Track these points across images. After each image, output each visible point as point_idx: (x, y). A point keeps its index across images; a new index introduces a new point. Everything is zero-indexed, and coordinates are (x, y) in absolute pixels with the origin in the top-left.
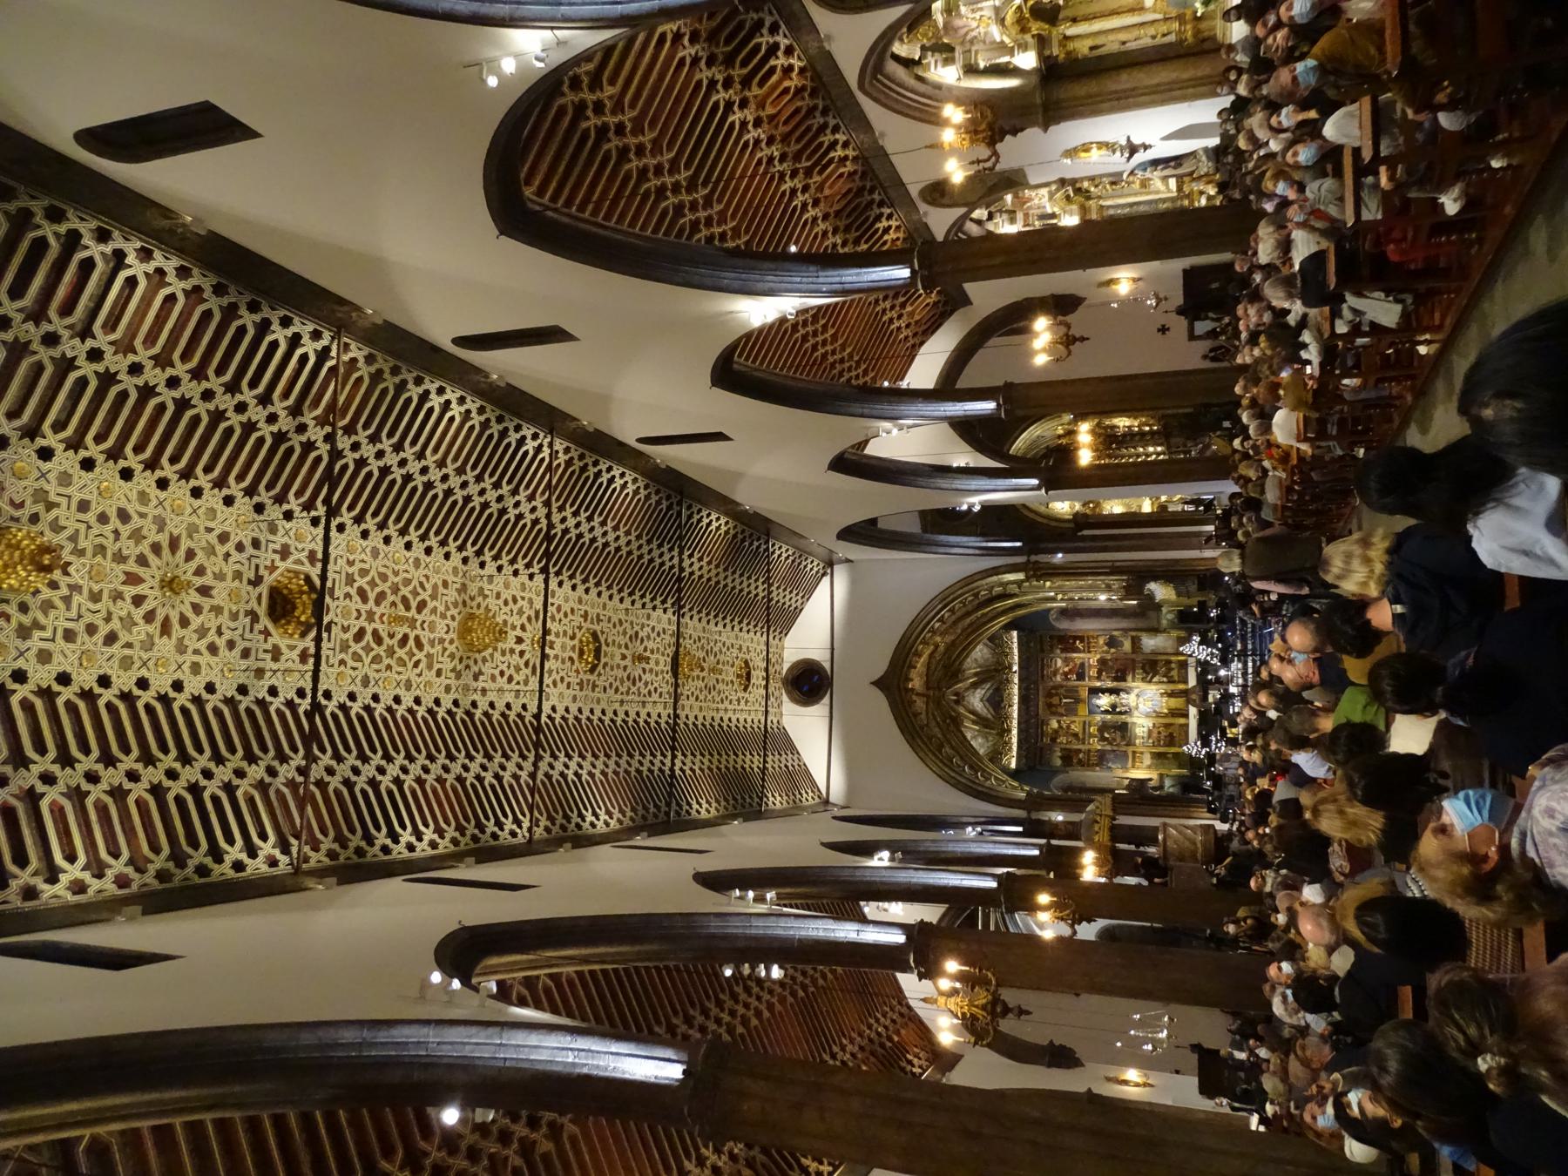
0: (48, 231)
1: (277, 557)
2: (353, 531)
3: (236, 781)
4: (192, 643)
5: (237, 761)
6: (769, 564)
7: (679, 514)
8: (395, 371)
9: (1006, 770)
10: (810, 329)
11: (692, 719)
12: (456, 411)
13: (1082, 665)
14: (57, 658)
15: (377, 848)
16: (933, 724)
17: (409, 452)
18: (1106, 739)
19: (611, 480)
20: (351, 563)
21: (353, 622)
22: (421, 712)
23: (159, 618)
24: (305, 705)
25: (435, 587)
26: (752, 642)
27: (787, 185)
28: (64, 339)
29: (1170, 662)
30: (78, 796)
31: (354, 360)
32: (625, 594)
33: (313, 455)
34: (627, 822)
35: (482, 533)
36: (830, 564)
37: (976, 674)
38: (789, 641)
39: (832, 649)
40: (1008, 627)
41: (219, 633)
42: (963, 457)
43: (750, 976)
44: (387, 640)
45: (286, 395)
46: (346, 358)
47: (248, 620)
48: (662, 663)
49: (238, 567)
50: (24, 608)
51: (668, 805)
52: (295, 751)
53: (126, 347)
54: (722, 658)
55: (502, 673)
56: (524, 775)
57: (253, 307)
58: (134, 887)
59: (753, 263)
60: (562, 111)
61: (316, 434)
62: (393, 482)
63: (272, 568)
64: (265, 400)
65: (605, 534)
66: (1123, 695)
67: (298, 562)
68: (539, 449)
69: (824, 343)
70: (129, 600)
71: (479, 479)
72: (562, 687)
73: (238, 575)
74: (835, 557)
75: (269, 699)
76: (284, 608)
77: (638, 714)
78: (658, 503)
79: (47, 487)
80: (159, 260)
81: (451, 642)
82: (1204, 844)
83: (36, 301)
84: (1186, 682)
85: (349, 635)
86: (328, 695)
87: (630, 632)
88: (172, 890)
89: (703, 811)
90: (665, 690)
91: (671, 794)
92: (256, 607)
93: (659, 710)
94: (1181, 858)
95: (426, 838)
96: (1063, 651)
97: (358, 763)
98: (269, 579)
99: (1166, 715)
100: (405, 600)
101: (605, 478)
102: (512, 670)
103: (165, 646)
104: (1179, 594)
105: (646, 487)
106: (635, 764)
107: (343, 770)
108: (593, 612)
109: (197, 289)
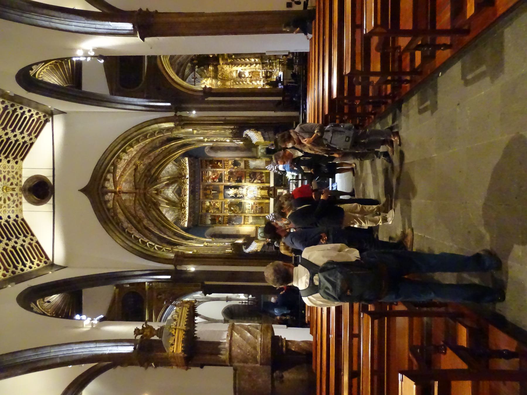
13: (221, 174)
18: (232, 210)
29: (262, 173)
36: (51, 114)
37: (168, 180)
40: (184, 155)
66: (240, 189)
82: (263, 346)
84: (269, 183)
96: (212, 167)
99: (260, 199)
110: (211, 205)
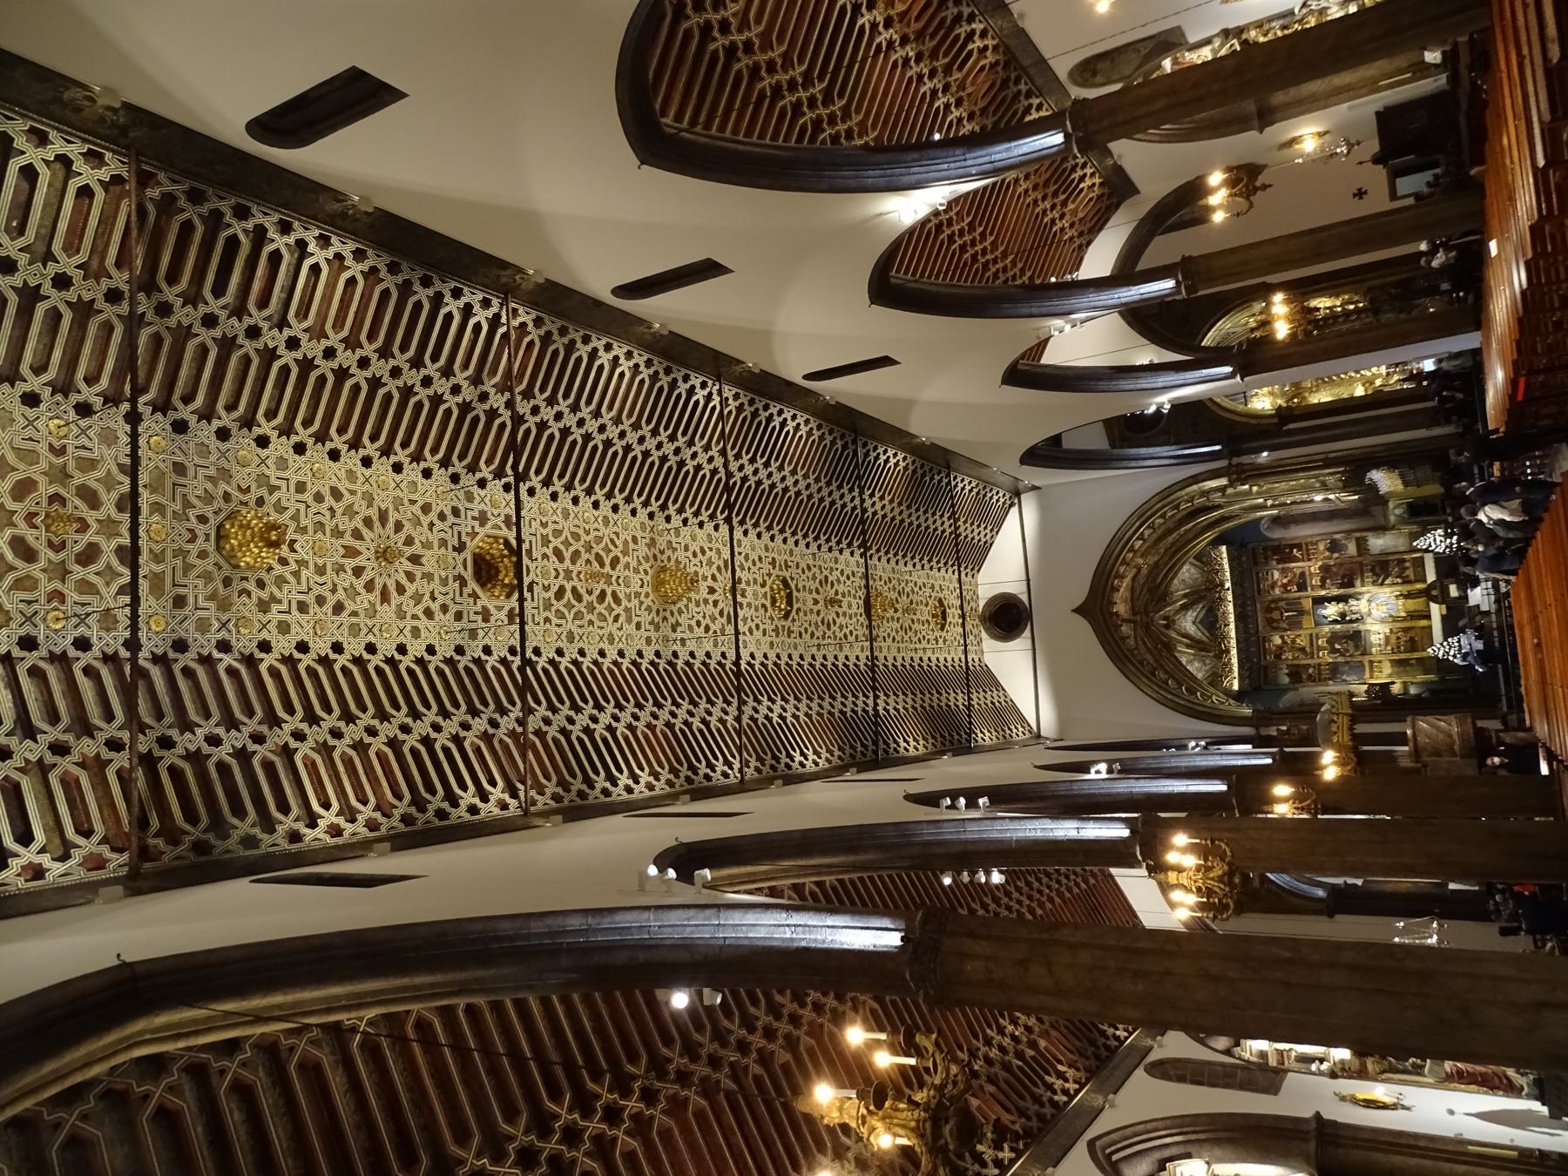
0: (239, 229)
1: (476, 523)
2: (543, 494)
3: (463, 734)
4: (410, 609)
5: (461, 714)
6: (952, 498)
7: (855, 452)
8: (563, 331)
9: (1228, 693)
10: (967, 238)
11: (891, 660)
12: (625, 366)
13: (1303, 574)
14: (294, 629)
15: (598, 791)
16: (1143, 650)
17: (585, 412)
19: (783, 424)
20: (545, 525)
21: (552, 581)
22: (626, 663)
23: (378, 587)
24: (516, 662)
25: (626, 542)
26: (944, 580)
27: (927, 86)
28: (264, 331)
29: (1404, 561)
30: (325, 750)
31: (523, 325)
32: (810, 539)
33: (497, 422)
34: (835, 761)
35: (664, 487)
36: (1018, 494)
37: (1185, 596)
38: (982, 577)
39: (1028, 580)
40: (1216, 542)
41: (434, 599)
42: (1148, 354)
43: (971, 882)
44: (586, 597)
45: (465, 366)
46: (515, 323)
47: (457, 584)
48: (854, 606)
49: (442, 535)
50: (261, 584)
51: (875, 743)
52: (514, 704)
53: (318, 333)
54: (915, 598)
55: (699, 624)
56: (730, 719)
57: (426, 282)
58: (383, 830)
59: (896, 157)
60: (688, 34)
61: (497, 401)
62: (574, 442)
63: (474, 534)
64: (447, 372)
65: (783, 479)
66: (1352, 602)
67: (496, 527)
68: (709, 398)
69: (984, 252)
70: (350, 572)
71: (655, 433)
72: (758, 634)
73: (443, 543)
74: (1021, 486)
75: (484, 657)
76: (488, 572)
77: (836, 657)
78: (833, 443)
79: (267, 472)
80: (336, 245)
81: (647, 595)
82: (1461, 735)
83: (237, 297)
84: (1425, 581)
85: (551, 594)
86: (537, 651)
87: (819, 577)
88: (415, 833)
89: (911, 749)
90: (860, 633)
91: (876, 733)
92: (463, 573)
93: (857, 652)
94: (1437, 753)
95: (642, 781)
97: (572, 713)
98: (471, 545)
99: (1405, 619)
100: (599, 558)
101: (777, 422)
102: (708, 621)
103: (387, 612)
104: (1406, 483)
105: (819, 427)
106: (838, 705)
107: (559, 720)
108: (780, 559)
109: (374, 270)
110: (1284, 642)
